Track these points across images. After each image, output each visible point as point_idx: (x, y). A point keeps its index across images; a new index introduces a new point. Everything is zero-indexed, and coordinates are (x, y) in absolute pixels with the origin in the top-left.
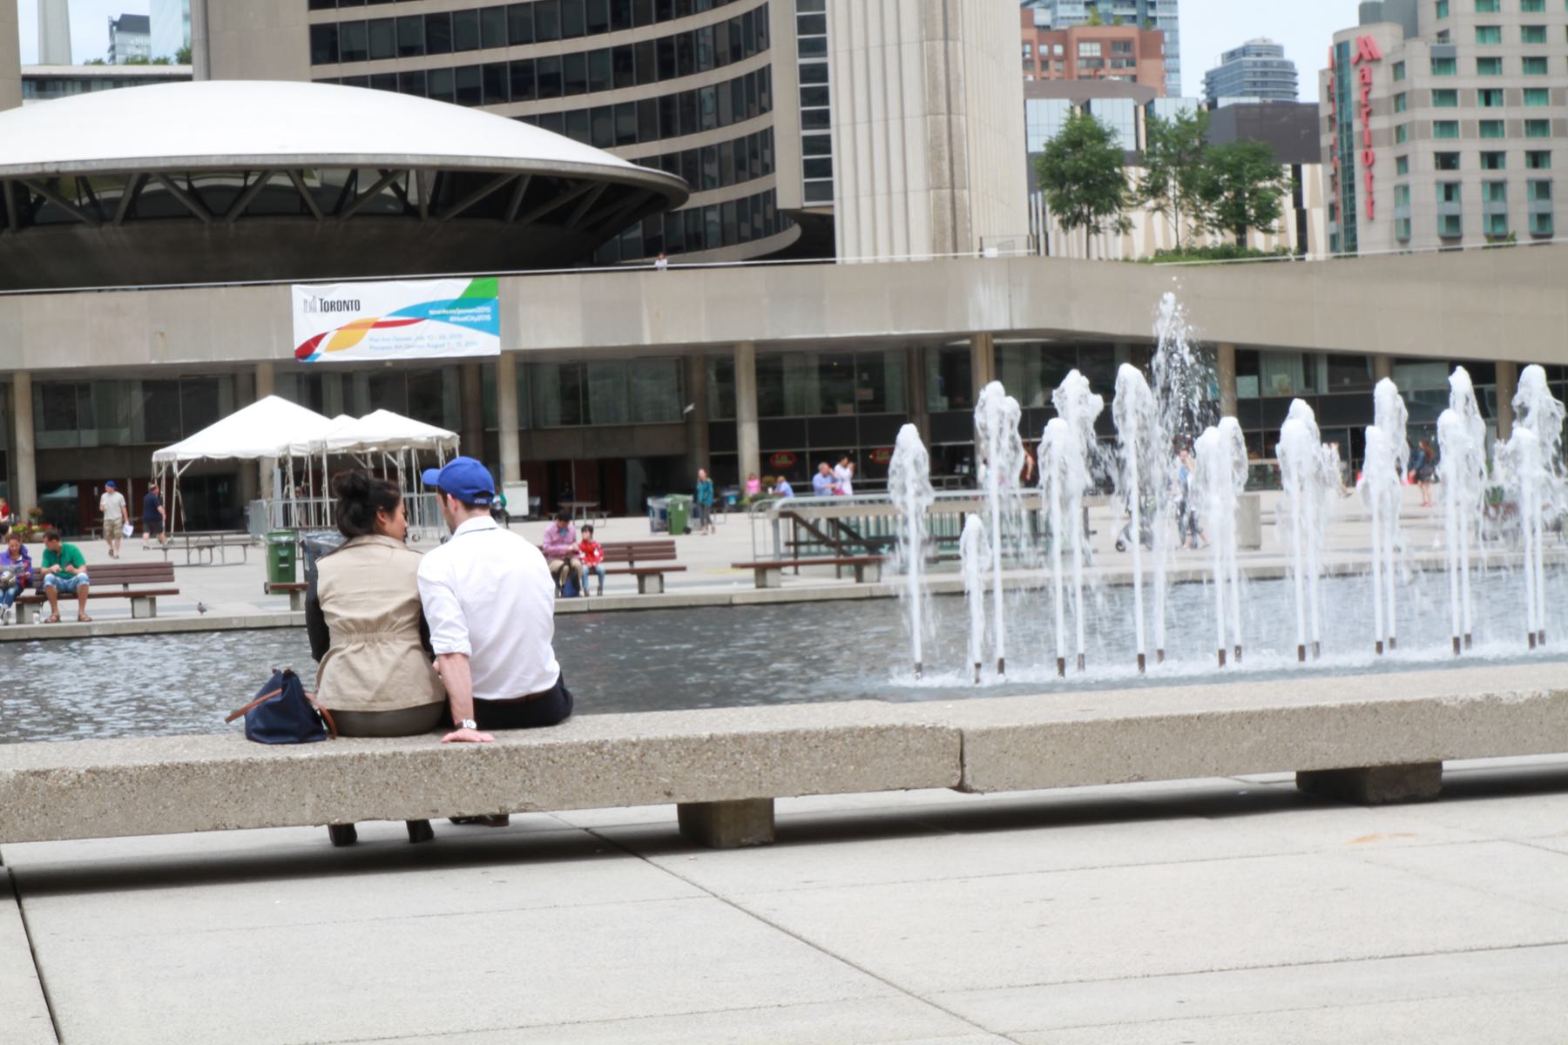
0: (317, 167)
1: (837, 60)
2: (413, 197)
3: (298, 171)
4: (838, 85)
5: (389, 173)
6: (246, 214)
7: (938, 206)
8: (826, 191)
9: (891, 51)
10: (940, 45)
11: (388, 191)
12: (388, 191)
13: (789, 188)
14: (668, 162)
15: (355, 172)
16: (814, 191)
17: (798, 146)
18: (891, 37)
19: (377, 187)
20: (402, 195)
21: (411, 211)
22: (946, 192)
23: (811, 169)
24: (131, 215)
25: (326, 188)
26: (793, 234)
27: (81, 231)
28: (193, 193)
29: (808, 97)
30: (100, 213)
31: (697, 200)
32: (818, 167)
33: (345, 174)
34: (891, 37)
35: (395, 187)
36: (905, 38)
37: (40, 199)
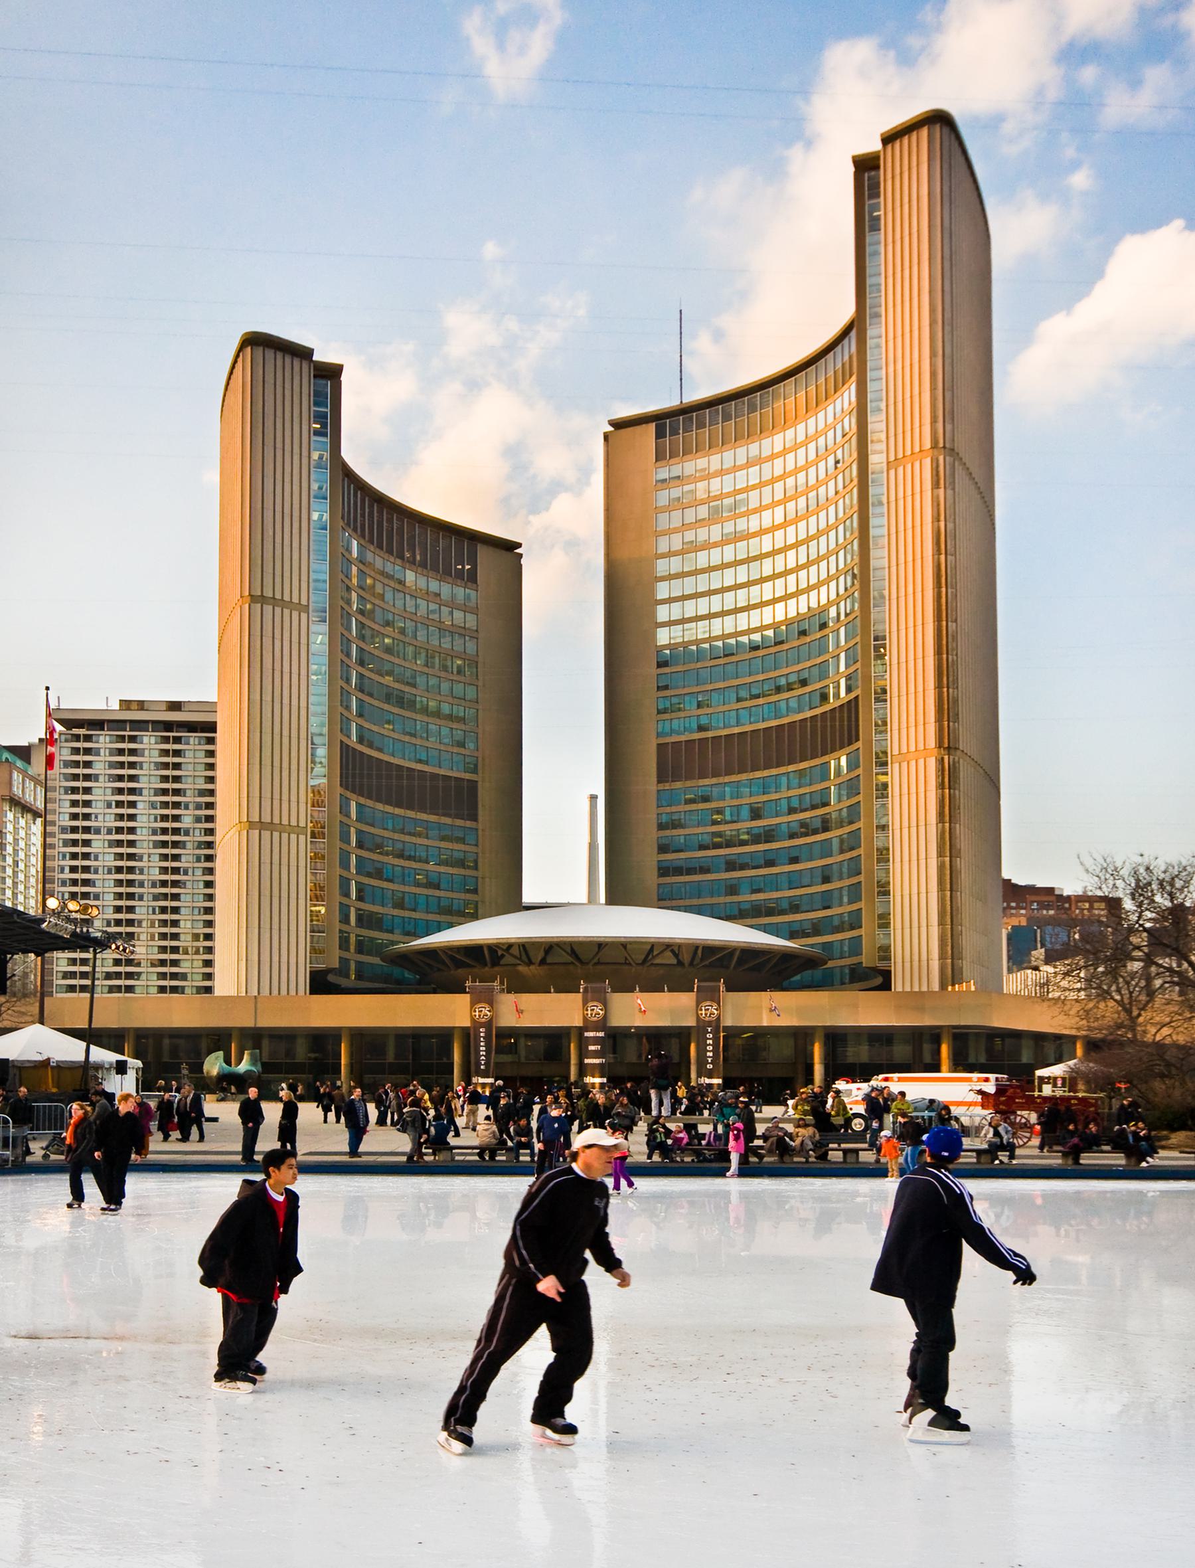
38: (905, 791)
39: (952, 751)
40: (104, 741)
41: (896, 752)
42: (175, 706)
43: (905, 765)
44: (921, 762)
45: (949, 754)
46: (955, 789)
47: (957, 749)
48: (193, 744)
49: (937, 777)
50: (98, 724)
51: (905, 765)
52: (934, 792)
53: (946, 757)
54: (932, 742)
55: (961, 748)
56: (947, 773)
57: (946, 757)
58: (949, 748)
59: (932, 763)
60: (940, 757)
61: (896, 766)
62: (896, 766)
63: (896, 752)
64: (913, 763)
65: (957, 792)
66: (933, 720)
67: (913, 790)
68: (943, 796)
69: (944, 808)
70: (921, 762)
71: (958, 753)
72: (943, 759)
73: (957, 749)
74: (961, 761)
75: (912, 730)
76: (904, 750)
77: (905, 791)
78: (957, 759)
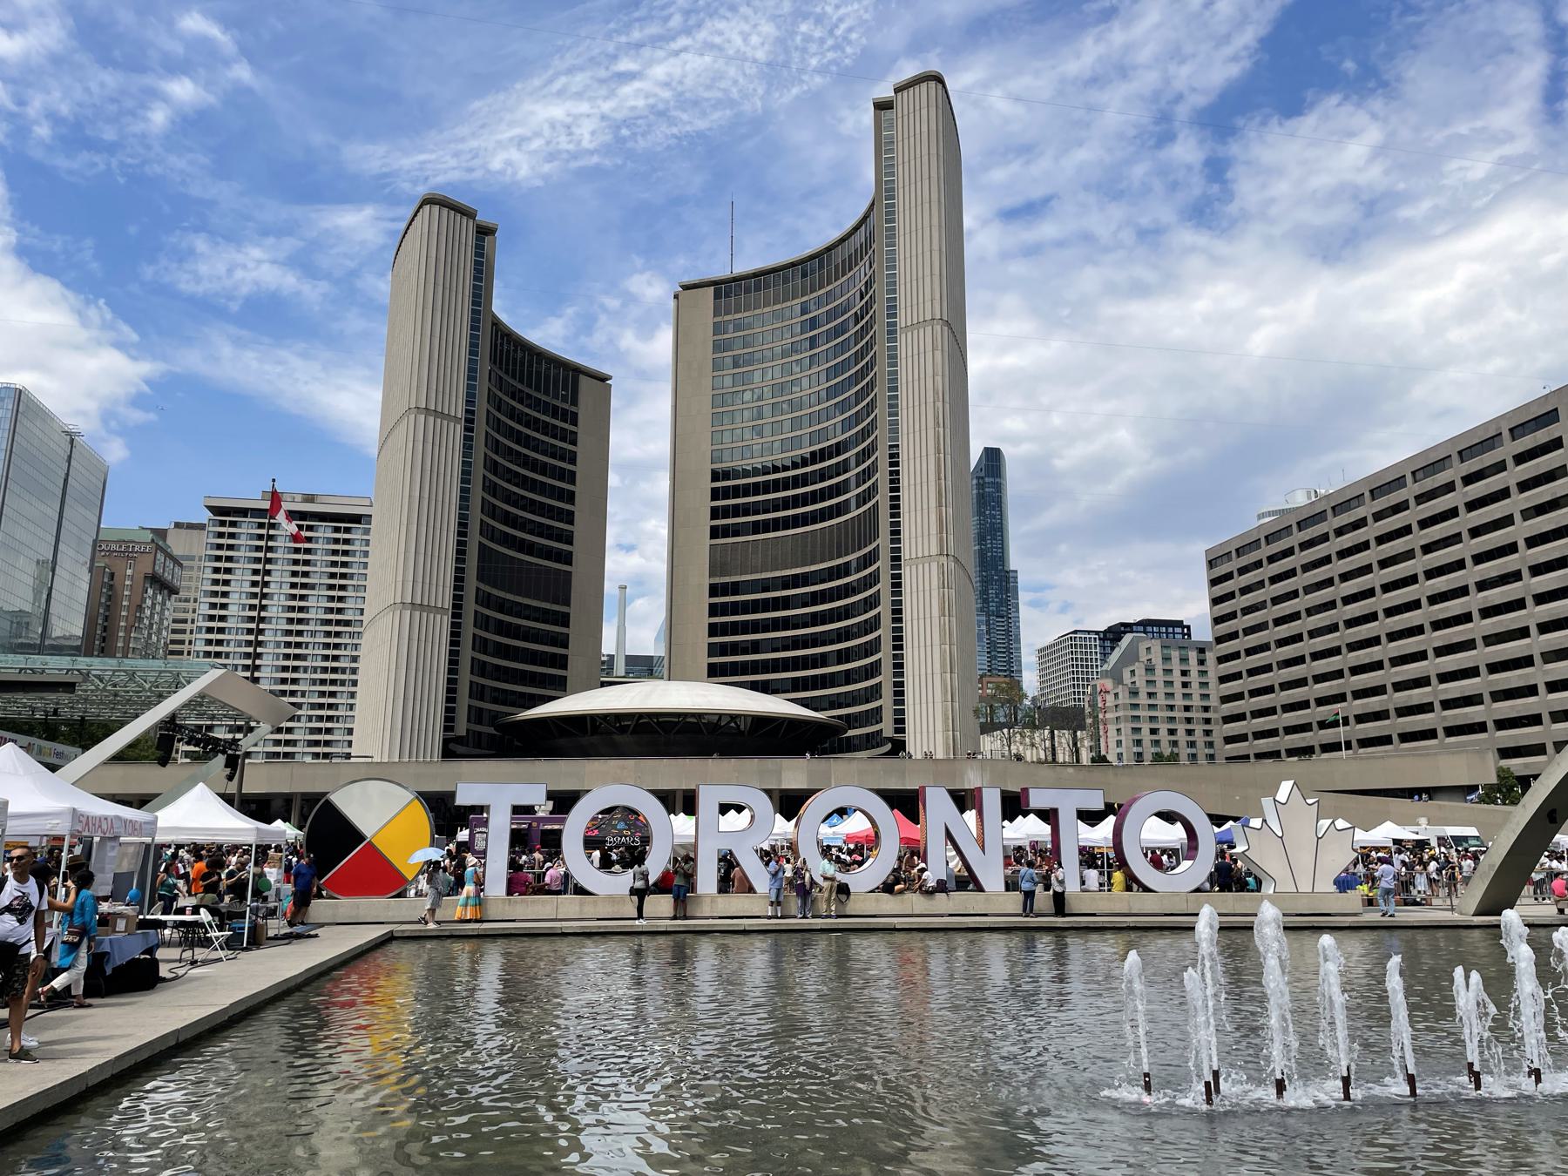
0: (706, 714)
1: (908, 680)
2: (742, 727)
3: (699, 715)
4: (908, 689)
5: (734, 717)
6: (678, 732)
7: (947, 738)
8: (903, 731)
9: (930, 677)
10: (948, 675)
11: (733, 724)
12: (733, 724)
13: (887, 727)
14: (839, 717)
15: (721, 716)
16: (897, 731)
17: (892, 712)
18: (929, 671)
19: (729, 723)
20: (738, 726)
21: (741, 733)
22: (951, 733)
23: (897, 721)
24: (634, 732)
25: (709, 723)
26: (888, 747)
27: (618, 738)
28: (659, 723)
29: (896, 693)
30: (623, 730)
31: (851, 733)
32: (900, 722)
33: (717, 717)
34: (929, 671)
35: (736, 723)
36: (935, 671)
37: (601, 724)
38: (915, 589)
40: (247, 527)
42: (310, 499)
43: (914, 568)
44: (927, 565)
48: (324, 531)
50: (244, 512)
54: (934, 550)
58: (947, 555)
59: (934, 566)
61: (908, 568)
62: (908, 568)
63: (907, 557)
64: (920, 567)
67: (921, 588)
70: (927, 565)
75: (920, 539)
76: (914, 556)
77: (915, 589)
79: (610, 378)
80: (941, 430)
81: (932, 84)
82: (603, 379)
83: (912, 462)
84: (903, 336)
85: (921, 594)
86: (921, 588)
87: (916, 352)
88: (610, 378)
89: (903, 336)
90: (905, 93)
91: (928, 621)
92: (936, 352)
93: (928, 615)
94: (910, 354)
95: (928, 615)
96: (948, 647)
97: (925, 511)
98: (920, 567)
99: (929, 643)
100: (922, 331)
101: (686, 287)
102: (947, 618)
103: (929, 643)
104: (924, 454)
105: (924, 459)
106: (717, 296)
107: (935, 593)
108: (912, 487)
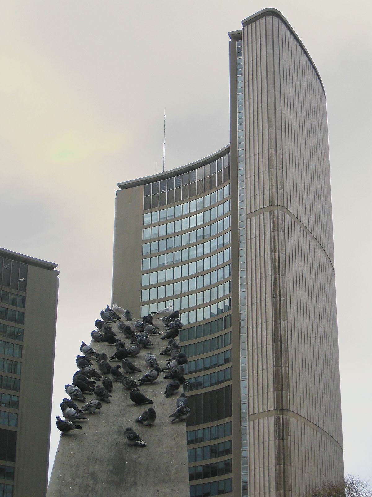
39: (285, 412)
41: (251, 413)
43: (256, 422)
44: (266, 419)
45: (283, 414)
46: (287, 440)
47: (288, 410)
49: (275, 431)
51: (256, 422)
52: (273, 442)
53: (281, 416)
54: (272, 407)
55: (291, 409)
56: (281, 428)
57: (281, 416)
59: (272, 419)
60: (277, 416)
64: (261, 420)
65: (289, 442)
66: (272, 389)
67: (261, 441)
68: (279, 445)
69: (280, 453)
70: (266, 419)
71: (290, 413)
72: (279, 418)
73: (288, 410)
74: (292, 419)
75: (261, 396)
76: (256, 412)
78: (288, 417)
79: (56, 266)
80: (278, 298)
81: (269, 18)
82: (50, 267)
83: (255, 328)
84: (249, 221)
85: (261, 445)
86: (261, 441)
87: (258, 234)
88: (56, 266)
89: (249, 221)
90: (250, 27)
91: (267, 469)
92: (272, 233)
93: (267, 465)
94: (253, 236)
95: (267, 465)
96: (282, 492)
97: (265, 371)
98: (261, 420)
99: (267, 490)
100: (262, 216)
101: (124, 186)
102: (282, 466)
103: (267, 490)
104: (264, 321)
105: (264, 325)
106: (147, 192)
107: (272, 444)
108: (255, 351)
